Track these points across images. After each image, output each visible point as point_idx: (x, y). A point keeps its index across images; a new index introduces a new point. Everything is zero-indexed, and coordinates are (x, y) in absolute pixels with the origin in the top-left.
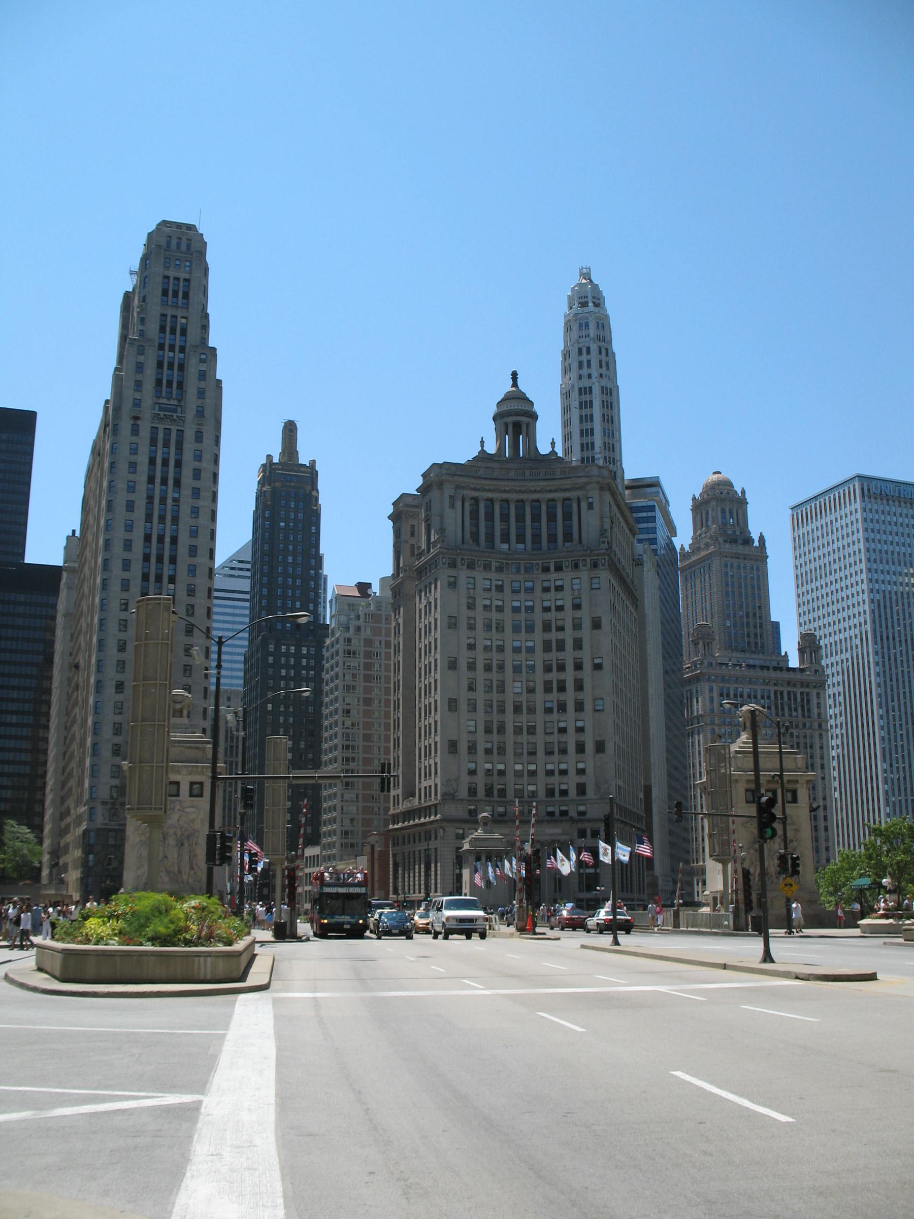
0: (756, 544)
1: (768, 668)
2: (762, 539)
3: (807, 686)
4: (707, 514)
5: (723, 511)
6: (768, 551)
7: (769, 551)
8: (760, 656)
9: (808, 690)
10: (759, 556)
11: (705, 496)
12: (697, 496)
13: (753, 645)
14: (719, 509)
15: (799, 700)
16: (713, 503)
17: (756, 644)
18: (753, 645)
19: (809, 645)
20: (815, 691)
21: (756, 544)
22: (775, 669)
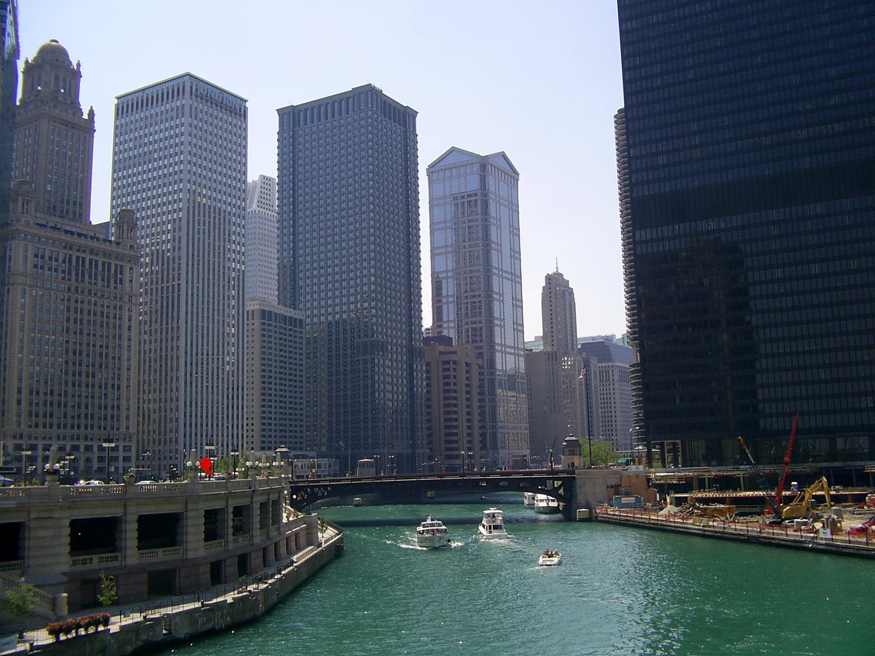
0: (85, 116)
1: (86, 236)
2: (91, 113)
3: (122, 260)
4: (39, 79)
5: (57, 78)
6: (95, 125)
7: (97, 126)
8: (78, 224)
9: (122, 263)
10: (88, 128)
11: (40, 60)
12: (30, 61)
13: (71, 213)
14: (53, 74)
15: (113, 272)
16: (48, 68)
17: (75, 212)
18: (71, 213)
19: (124, 218)
20: (128, 266)
21: (85, 116)
22: (92, 238)
